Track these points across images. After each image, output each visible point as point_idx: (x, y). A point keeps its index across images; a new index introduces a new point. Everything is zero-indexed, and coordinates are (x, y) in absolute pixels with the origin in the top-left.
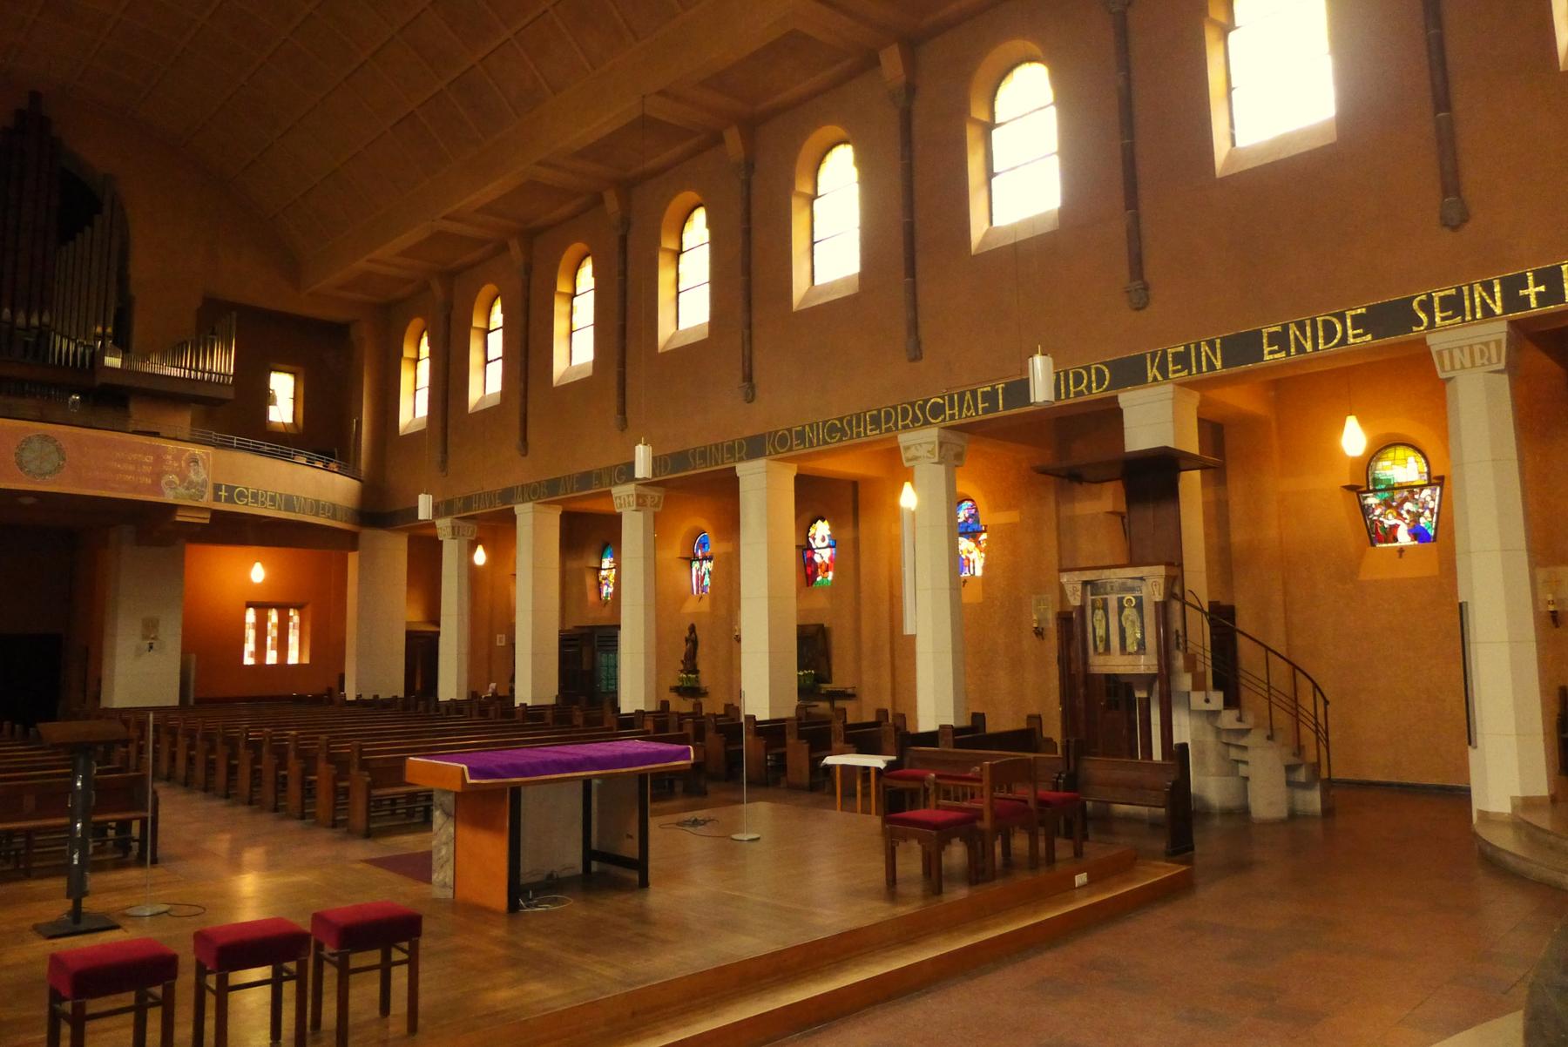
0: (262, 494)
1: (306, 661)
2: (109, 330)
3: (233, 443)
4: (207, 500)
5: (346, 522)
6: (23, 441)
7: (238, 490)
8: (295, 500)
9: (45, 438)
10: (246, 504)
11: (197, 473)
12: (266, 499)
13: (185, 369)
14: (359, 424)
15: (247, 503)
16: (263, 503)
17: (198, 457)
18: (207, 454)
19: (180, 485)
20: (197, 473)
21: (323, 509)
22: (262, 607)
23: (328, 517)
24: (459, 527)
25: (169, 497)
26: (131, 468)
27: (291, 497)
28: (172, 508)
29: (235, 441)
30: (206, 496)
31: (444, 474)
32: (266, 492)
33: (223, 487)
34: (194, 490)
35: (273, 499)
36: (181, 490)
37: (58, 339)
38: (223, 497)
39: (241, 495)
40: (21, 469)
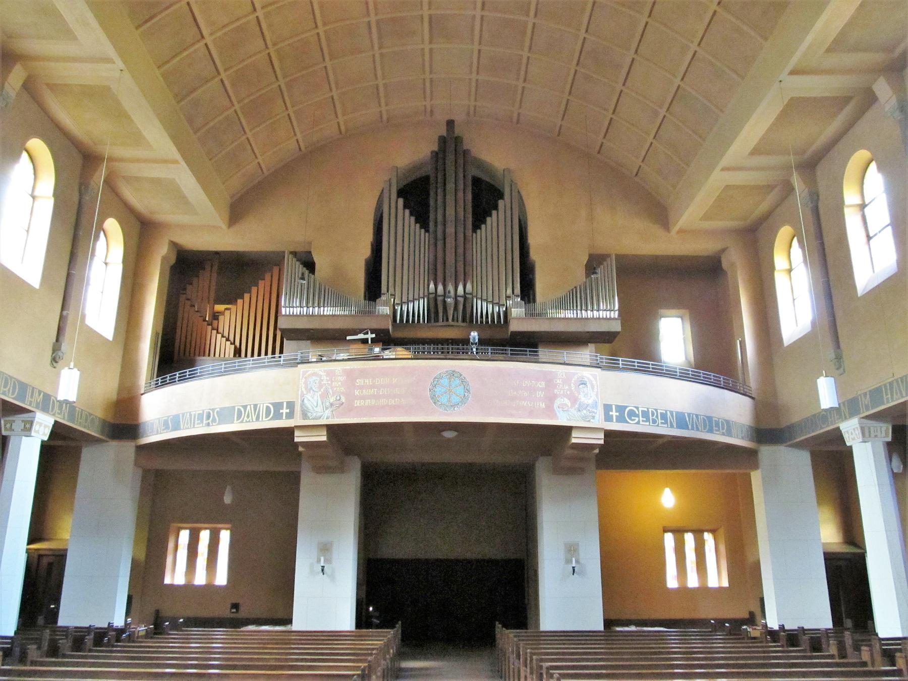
0: (652, 412)
1: (725, 583)
3: (619, 364)
4: (599, 421)
5: (743, 438)
6: (435, 378)
7: (627, 409)
8: (687, 417)
9: (452, 374)
10: (638, 423)
11: (586, 395)
12: (657, 417)
14: (743, 344)
15: (639, 421)
16: (654, 422)
17: (586, 379)
18: (595, 377)
19: (571, 407)
20: (586, 395)
21: (717, 425)
22: (678, 532)
23: (723, 434)
24: (869, 428)
25: (561, 420)
26: (526, 394)
27: (683, 414)
28: (567, 431)
29: (620, 362)
30: (597, 417)
31: (842, 370)
32: (656, 410)
34: (585, 412)
35: (664, 416)
36: (573, 411)
37: (479, 302)
38: (614, 418)
39: (632, 414)
40: (435, 403)
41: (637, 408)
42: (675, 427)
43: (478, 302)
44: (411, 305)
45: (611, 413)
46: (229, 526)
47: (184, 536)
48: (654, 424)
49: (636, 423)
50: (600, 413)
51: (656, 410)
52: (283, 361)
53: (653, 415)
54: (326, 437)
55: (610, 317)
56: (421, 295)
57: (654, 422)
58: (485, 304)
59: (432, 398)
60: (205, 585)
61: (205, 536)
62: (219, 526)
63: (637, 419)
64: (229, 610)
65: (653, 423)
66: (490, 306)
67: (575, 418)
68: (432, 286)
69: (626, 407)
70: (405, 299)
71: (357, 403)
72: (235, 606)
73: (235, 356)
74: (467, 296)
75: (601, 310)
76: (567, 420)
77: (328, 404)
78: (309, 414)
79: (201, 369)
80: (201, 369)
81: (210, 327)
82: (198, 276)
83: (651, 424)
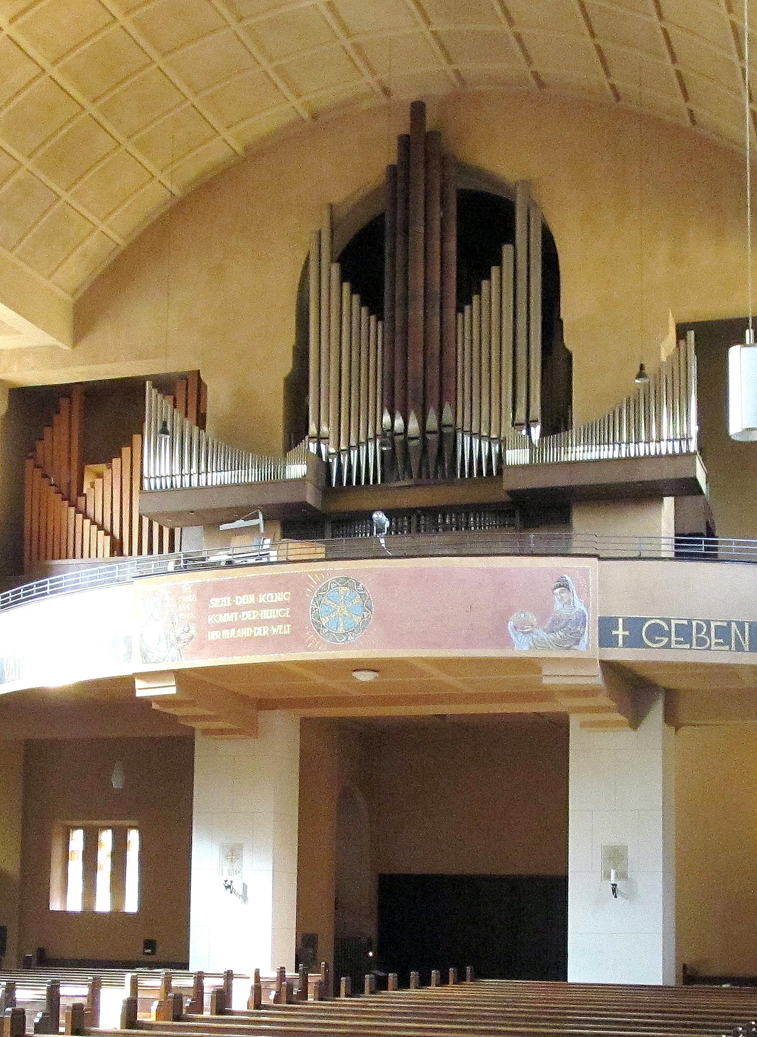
2: (536, 411)
7: (647, 624)
10: (668, 646)
12: (708, 633)
13: (628, 443)
25: (521, 647)
33: (621, 621)
35: (723, 633)
36: (541, 634)
37: (467, 439)
39: (656, 631)
40: (319, 631)
41: (668, 621)
42: (747, 649)
43: (465, 439)
44: (354, 454)
45: (614, 632)
46: (135, 823)
47: (77, 839)
48: (706, 642)
49: (662, 647)
50: (590, 635)
51: (708, 623)
52: (115, 573)
53: (699, 629)
54: (175, 688)
55: (688, 451)
56: (371, 435)
57: (701, 642)
58: (476, 442)
59: (315, 623)
60: (111, 913)
61: (106, 838)
62: (128, 823)
63: (666, 640)
64: (142, 951)
65: (697, 645)
66: (485, 445)
67: (544, 645)
68: (387, 418)
69: (646, 620)
70: (353, 443)
71: (213, 635)
72: (150, 944)
73: (112, 554)
74: (445, 430)
75: (652, 441)
76: (530, 648)
77: (173, 638)
78: (150, 655)
79: (51, 581)
80: (51, 581)
81: (72, 510)
82: (51, 425)
83: (694, 647)
